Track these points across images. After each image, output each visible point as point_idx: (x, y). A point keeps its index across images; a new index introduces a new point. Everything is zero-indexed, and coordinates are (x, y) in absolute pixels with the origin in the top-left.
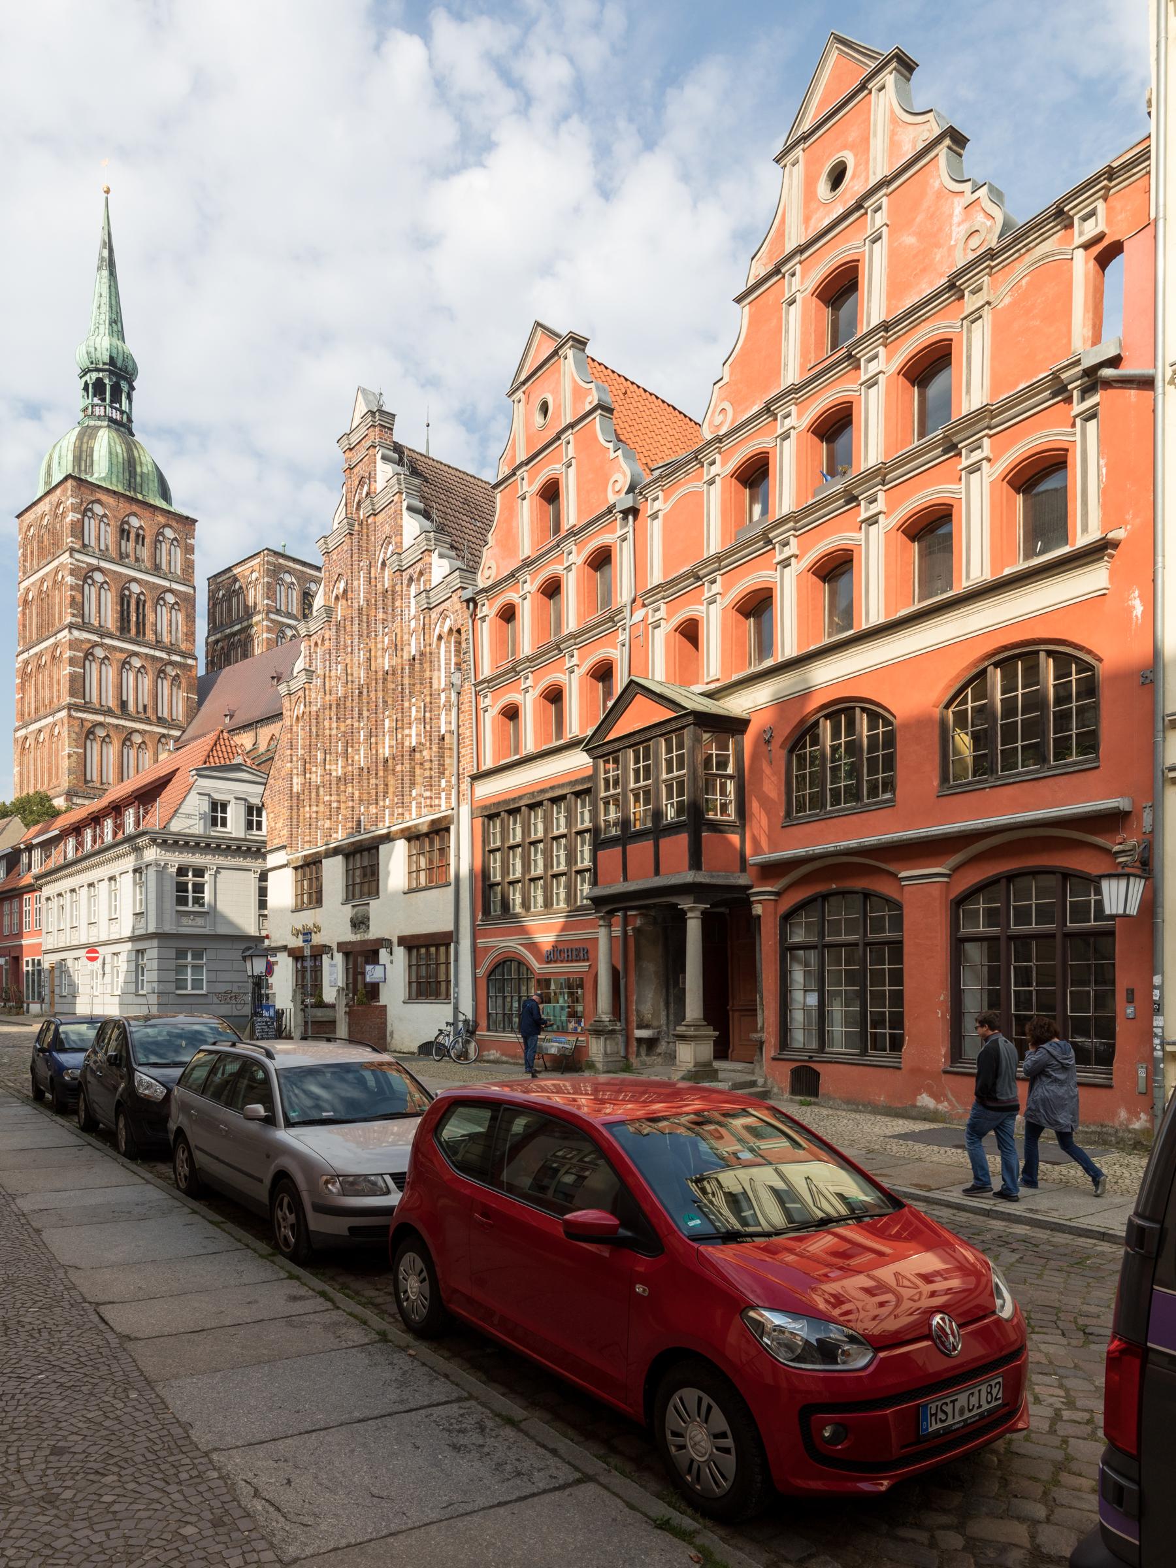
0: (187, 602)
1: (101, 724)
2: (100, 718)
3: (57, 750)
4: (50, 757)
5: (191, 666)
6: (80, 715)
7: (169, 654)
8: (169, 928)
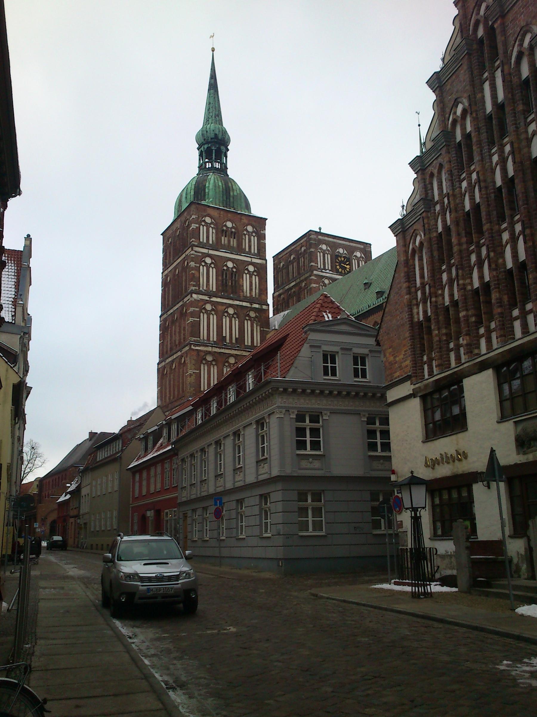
0: (261, 270)
1: (209, 353)
2: (210, 349)
3: (183, 373)
4: (179, 377)
6: (197, 348)
8: (288, 471)
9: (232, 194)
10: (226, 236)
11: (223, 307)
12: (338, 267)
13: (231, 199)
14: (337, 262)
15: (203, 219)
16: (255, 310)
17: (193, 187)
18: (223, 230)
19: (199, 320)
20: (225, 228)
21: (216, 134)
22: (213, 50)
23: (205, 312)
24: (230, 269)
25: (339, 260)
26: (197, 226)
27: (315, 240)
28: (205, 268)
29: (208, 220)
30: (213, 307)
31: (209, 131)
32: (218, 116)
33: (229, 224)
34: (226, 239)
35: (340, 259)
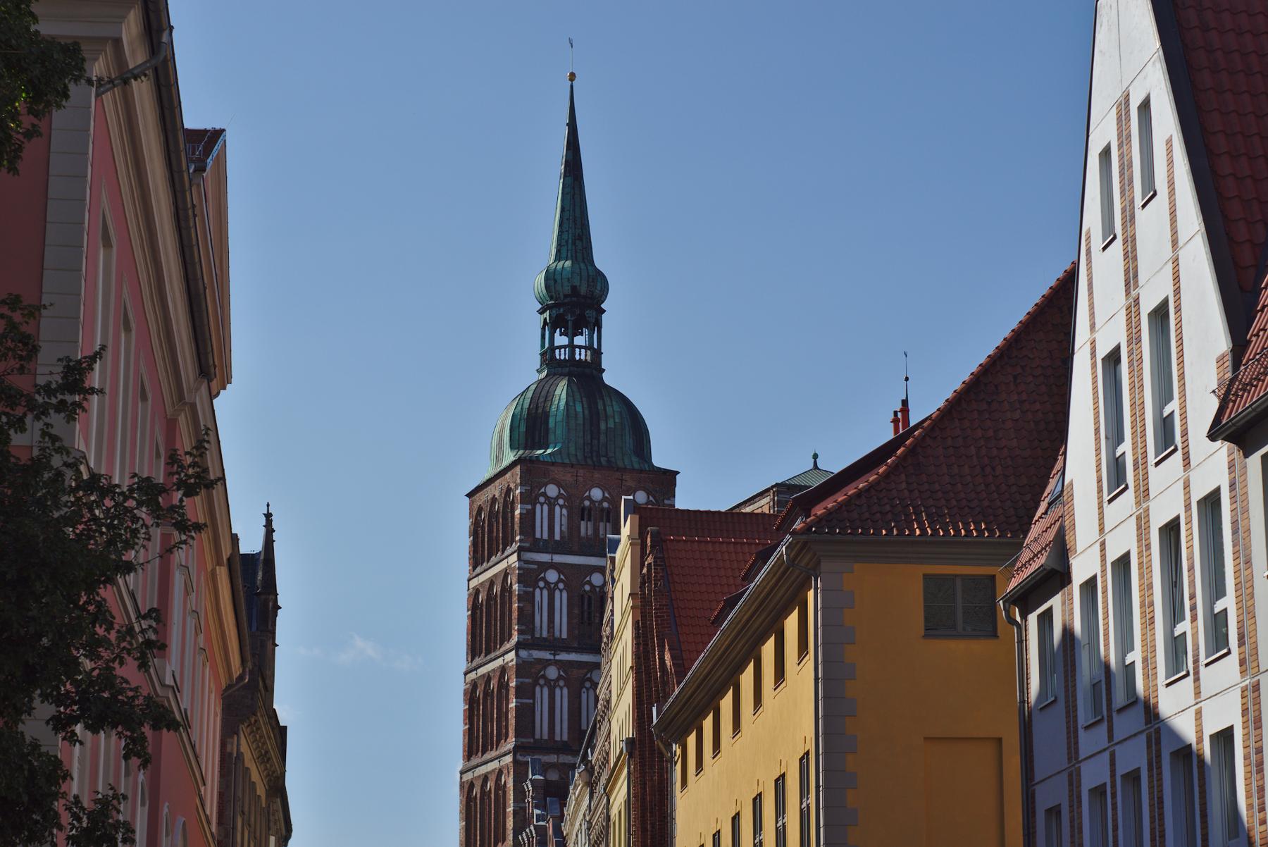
9: (603, 426)
10: (589, 520)
13: (602, 438)
18: (583, 509)
19: (531, 701)
20: (587, 503)
21: (574, 288)
22: (572, 77)
23: (545, 684)
24: (598, 589)
26: (529, 507)
28: (545, 592)
29: (552, 490)
30: (562, 673)
31: (559, 281)
32: (580, 238)
33: (597, 494)
34: (590, 525)
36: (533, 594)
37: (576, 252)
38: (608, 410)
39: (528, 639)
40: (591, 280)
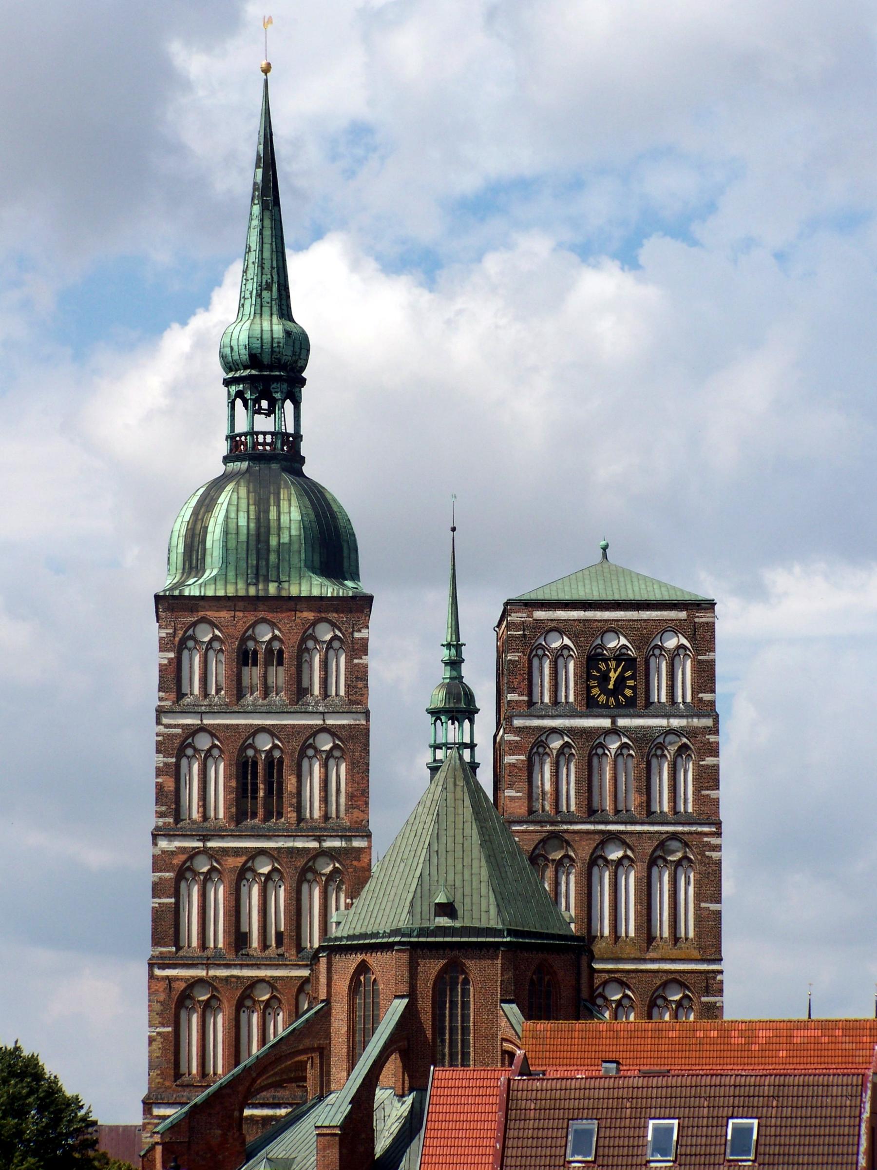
1: (200, 981)
5: (360, 850)
7: (319, 839)
9: (273, 542)
11: (239, 859)
12: (595, 691)
13: (273, 557)
14: (595, 678)
15: (190, 632)
16: (332, 854)
17: (183, 532)
19: (173, 900)
22: (266, 70)
25: (599, 670)
26: (172, 655)
27: (523, 626)
31: (235, 348)
35: (603, 666)
36: (178, 766)
37: (262, 306)
38: (282, 520)
39: (169, 823)
40: (275, 345)
